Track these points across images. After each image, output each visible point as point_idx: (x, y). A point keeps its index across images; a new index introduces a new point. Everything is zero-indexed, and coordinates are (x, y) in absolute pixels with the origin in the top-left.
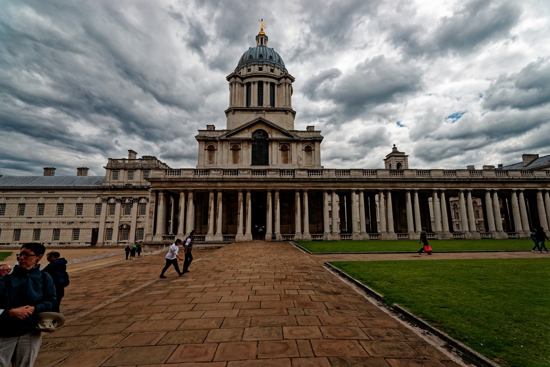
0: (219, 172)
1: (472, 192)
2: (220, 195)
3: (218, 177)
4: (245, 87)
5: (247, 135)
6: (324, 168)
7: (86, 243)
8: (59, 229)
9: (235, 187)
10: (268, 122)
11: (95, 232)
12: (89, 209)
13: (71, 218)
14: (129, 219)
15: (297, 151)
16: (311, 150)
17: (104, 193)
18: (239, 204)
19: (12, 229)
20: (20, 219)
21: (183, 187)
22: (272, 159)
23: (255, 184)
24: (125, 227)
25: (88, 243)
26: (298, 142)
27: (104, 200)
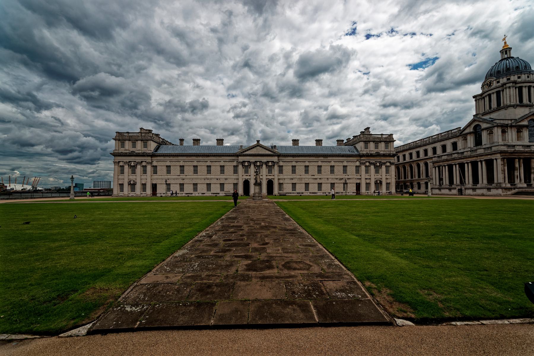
4: (517, 89)
5: (525, 123)
7: (353, 193)
8: (334, 183)
11: (358, 186)
12: (351, 169)
13: (341, 176)
14: (379, 177)
17: (362, 159)
19: (304, 183)
20: (307, 176)
21: (518, 156)
25: (354, 193)
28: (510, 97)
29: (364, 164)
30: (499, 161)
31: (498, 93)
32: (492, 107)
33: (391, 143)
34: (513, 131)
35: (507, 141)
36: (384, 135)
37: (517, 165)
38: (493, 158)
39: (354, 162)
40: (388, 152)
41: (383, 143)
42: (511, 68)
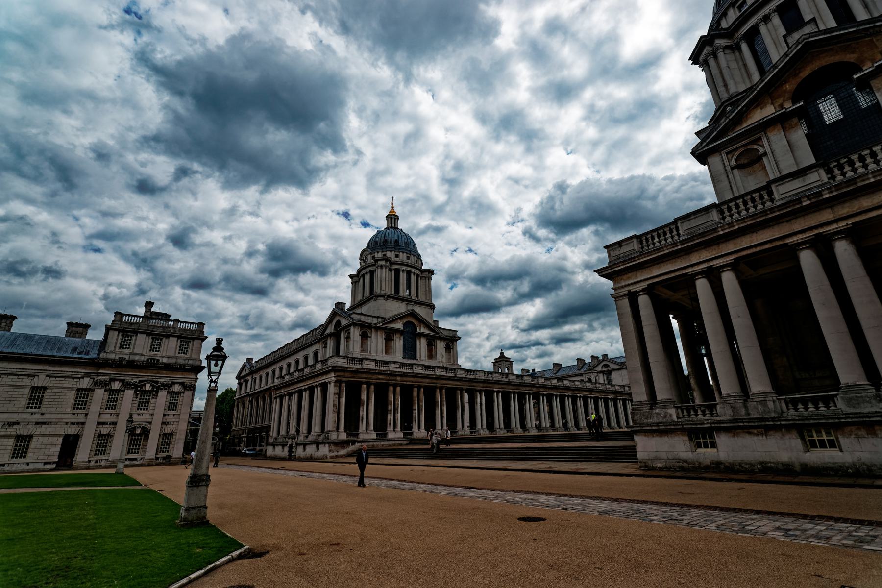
0: (398, 366)
1: (533, 394)
2: (398, 389)
3: (396, 370)
4: (393, 272)
5: (399, 325)
6: (462, 368)
7: (45, 463)
9: (412, 382)
10: (419, 315)
11: (70, 444)
13: (15, 416)
14: (147, 417)
15: (440, 346)
16: (450, 349)
17: (101, 371)
18: (414, 399)
21: (366, 378)
22: (420, 353)
23: (427, 380)
24: (138, 431)
25: (50, 463)
26: (441, 339)
27: (97, 384)
28: (381, 281)
29: (106, 384)
30: (332, 384)
31: (372, 273)
32: (365, 296)
33: (196, 341)
34: (379, 337)
35: (369, 354)
36: (181, 322)
37: (364, 397)
38: (327, 380)
39: (74, 378)
40: (181, 361)
41: (176, 339)
42: (389, 240)
